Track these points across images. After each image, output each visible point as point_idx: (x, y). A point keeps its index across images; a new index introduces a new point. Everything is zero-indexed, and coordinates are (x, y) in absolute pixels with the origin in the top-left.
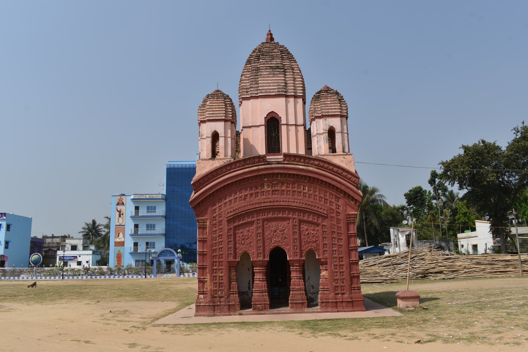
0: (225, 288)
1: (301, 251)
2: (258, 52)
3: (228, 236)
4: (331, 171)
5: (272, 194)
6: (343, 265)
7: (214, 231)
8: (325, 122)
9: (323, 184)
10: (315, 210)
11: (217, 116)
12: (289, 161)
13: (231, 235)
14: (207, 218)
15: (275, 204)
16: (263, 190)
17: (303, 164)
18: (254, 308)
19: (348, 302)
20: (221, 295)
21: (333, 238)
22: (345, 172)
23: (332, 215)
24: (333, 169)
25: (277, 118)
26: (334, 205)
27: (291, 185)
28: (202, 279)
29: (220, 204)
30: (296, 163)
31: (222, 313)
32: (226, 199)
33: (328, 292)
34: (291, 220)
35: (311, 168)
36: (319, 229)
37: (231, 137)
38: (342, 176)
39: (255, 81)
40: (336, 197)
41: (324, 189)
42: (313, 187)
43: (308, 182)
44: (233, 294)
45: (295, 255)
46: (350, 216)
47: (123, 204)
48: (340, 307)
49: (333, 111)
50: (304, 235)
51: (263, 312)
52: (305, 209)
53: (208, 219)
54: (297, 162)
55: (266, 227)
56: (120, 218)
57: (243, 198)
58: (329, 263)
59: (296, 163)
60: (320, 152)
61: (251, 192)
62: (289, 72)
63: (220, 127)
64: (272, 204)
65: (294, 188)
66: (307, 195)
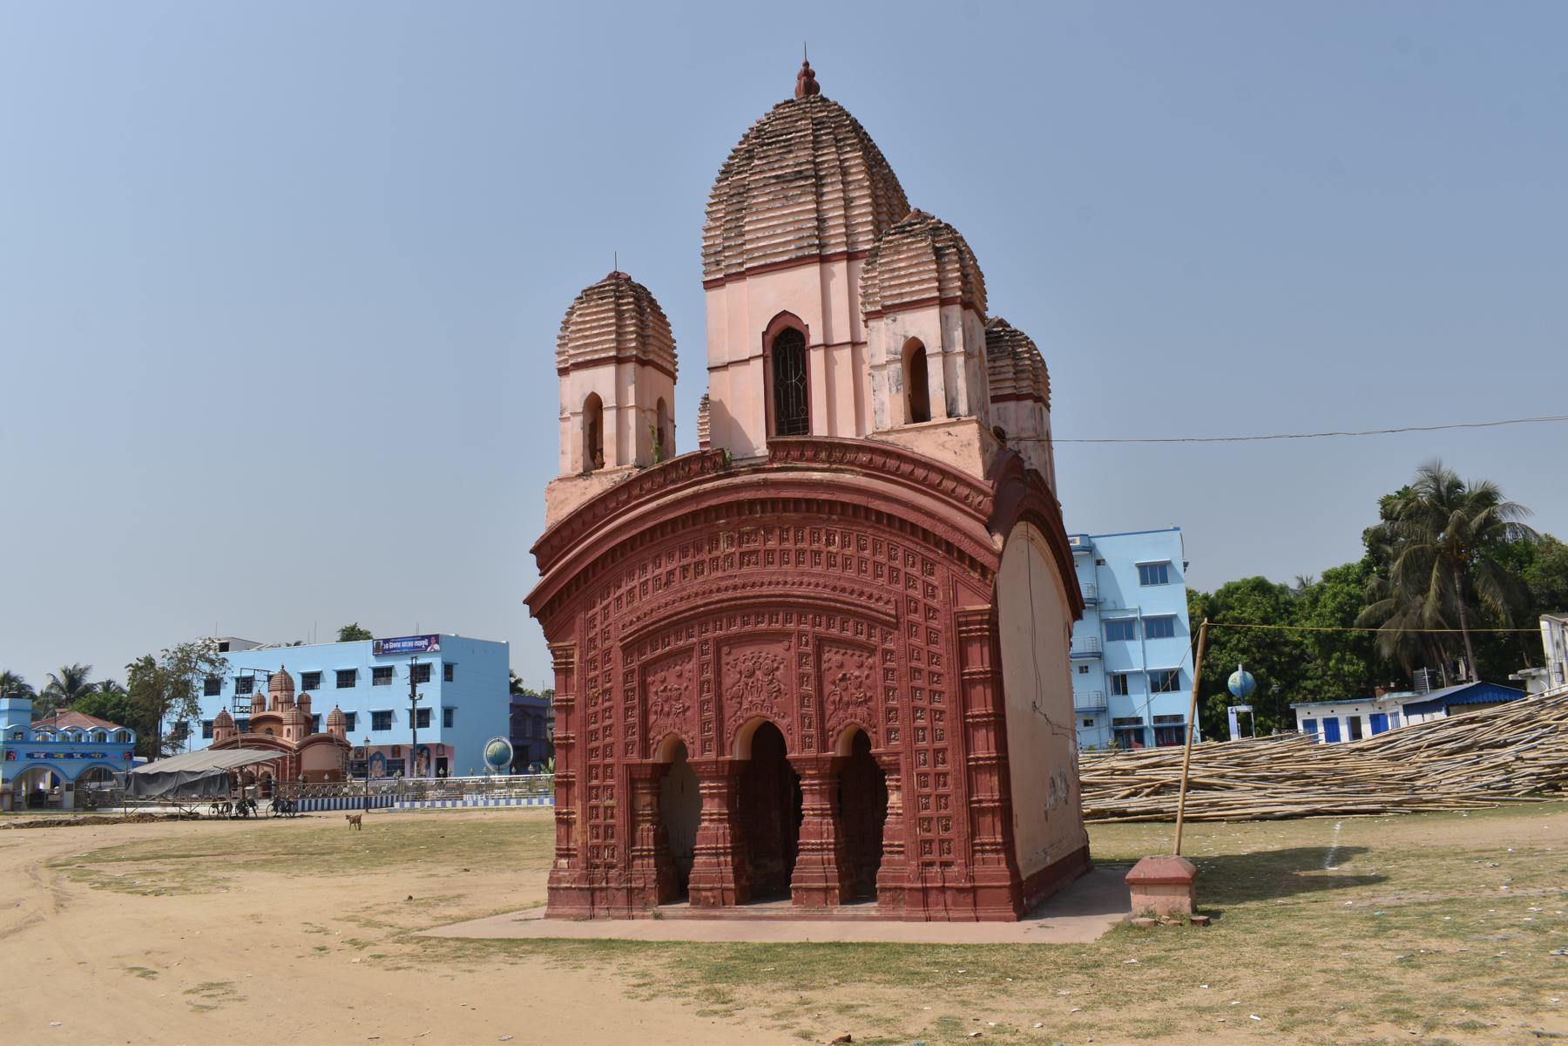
0: (619, 841)
1: (823, 732)
4: (908, 480)
5: (742, 564)
6: (945, 775)
7: (591, 680)
8: (893, 326)
10: (861, 606)
12: (785, 459)
13: (633, 690)
14: (573, 642)
15: (749, 592)
16: (715, 553)
17: (826, 466)
18: (694, 898)
19: (960, 890)
20: (610, 860)
21: (917, 689)
22: (949, 479)
24: (912, 472)
25: (797, 327)
28: (564, 814)
29: (605, 603)
30: (804, 465)
32: (619, 587)
33: (902, 857)
34: (794, 640)
35: (847, 478)
36: (875, 662)
37: (636, 407)
39: (736, 227)
41: (887, 536)
42: (855, 534)
43: (840, 520)
44: (642, 857)
45: (805, 745)
46: (969, 619)
48: (937, 905)
49: (917, 288)
50: (833, 683)
51: (718, 913)
52: (832, 604)
53: (575, 645)
54: (807, 460)
55: (728, 664)
57: (664, 581)
58: (903, 767)
59: (804, 465)
60: (881, 422)
61: (685, 562)
62: (832, 183)
63: (603, 381)
64: (738, 593)
65: (802, 540)
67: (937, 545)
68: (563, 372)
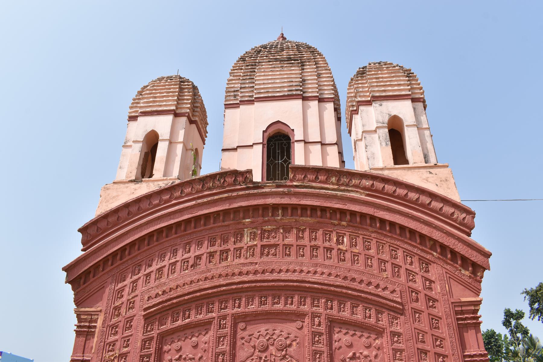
5: (262, 254)
7: (109, 344)
9: (385, 230)
10: (370, 294)
11: (160, 106)
14: (99, 309)
15: (267, 276)
16: (238, 245)
17: (336, 187)
22: (437, 201)
23: (414, 305)
24: (406, 195)
26: (418, 279)
27: (307, 234)
32: (150, 266)
34: (307, 320)
36: (382, 343)
40: (422, 260)
41: (388, 240)
43: (349, 226)
46: (464, 308)
49: (396, 88)
53: (101, 311)
54: (320, 182)
55: (243, 338)
61: (212, 249)
64: (259, 277)
66: (348, 256)
67: (433, 248)
68: (132, 118)
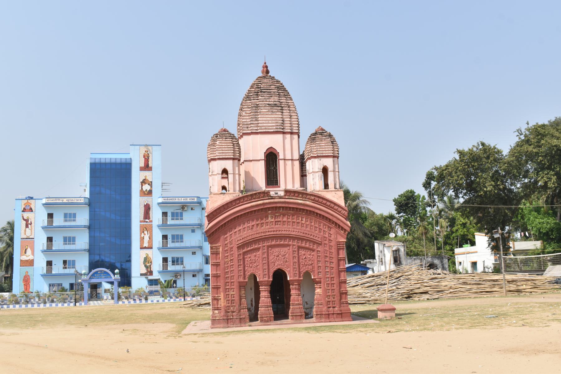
0: (237, 303)
1: (300, 273)
2: (256, 88)
3: (238, 260)
4: (325, 205)
5: (275, 224)
6: (334, 284)
9: (318, 216)
10: (311, 238)
12: (289, 196)
13: (241, 260)
14: (219, 245)
15: (278, 233)
16: (267, 221)
17: (301, 199)
20: (233, 310)
23: (325, 242)
26: (327, 233)
27: (291, 217)
29: (231, 233)
30: (295, 198)
31: (234, 325)
33: (322, 306)
34: (291, 247)
35: (308, 203)
38: (334, 209)
40: (329, 227)
41: (318, 220)
43: (305, 214)
47: (31, 210)
49: (327, 152)
50: (302, 259)
54: (296, 197)
56: (27, 229)
57: (251, 228)
58: (322, 282)
59: (295, 198)
61: (258, 223)
64: (275, 233)
65: (294, 219)
66: (305, 225)
67: (333, 223)
